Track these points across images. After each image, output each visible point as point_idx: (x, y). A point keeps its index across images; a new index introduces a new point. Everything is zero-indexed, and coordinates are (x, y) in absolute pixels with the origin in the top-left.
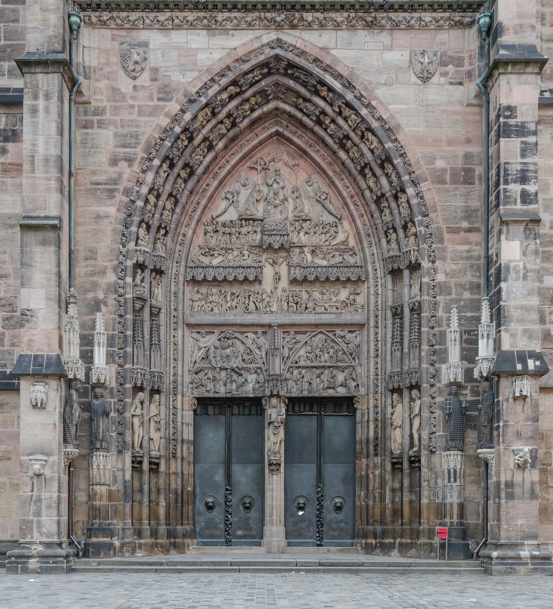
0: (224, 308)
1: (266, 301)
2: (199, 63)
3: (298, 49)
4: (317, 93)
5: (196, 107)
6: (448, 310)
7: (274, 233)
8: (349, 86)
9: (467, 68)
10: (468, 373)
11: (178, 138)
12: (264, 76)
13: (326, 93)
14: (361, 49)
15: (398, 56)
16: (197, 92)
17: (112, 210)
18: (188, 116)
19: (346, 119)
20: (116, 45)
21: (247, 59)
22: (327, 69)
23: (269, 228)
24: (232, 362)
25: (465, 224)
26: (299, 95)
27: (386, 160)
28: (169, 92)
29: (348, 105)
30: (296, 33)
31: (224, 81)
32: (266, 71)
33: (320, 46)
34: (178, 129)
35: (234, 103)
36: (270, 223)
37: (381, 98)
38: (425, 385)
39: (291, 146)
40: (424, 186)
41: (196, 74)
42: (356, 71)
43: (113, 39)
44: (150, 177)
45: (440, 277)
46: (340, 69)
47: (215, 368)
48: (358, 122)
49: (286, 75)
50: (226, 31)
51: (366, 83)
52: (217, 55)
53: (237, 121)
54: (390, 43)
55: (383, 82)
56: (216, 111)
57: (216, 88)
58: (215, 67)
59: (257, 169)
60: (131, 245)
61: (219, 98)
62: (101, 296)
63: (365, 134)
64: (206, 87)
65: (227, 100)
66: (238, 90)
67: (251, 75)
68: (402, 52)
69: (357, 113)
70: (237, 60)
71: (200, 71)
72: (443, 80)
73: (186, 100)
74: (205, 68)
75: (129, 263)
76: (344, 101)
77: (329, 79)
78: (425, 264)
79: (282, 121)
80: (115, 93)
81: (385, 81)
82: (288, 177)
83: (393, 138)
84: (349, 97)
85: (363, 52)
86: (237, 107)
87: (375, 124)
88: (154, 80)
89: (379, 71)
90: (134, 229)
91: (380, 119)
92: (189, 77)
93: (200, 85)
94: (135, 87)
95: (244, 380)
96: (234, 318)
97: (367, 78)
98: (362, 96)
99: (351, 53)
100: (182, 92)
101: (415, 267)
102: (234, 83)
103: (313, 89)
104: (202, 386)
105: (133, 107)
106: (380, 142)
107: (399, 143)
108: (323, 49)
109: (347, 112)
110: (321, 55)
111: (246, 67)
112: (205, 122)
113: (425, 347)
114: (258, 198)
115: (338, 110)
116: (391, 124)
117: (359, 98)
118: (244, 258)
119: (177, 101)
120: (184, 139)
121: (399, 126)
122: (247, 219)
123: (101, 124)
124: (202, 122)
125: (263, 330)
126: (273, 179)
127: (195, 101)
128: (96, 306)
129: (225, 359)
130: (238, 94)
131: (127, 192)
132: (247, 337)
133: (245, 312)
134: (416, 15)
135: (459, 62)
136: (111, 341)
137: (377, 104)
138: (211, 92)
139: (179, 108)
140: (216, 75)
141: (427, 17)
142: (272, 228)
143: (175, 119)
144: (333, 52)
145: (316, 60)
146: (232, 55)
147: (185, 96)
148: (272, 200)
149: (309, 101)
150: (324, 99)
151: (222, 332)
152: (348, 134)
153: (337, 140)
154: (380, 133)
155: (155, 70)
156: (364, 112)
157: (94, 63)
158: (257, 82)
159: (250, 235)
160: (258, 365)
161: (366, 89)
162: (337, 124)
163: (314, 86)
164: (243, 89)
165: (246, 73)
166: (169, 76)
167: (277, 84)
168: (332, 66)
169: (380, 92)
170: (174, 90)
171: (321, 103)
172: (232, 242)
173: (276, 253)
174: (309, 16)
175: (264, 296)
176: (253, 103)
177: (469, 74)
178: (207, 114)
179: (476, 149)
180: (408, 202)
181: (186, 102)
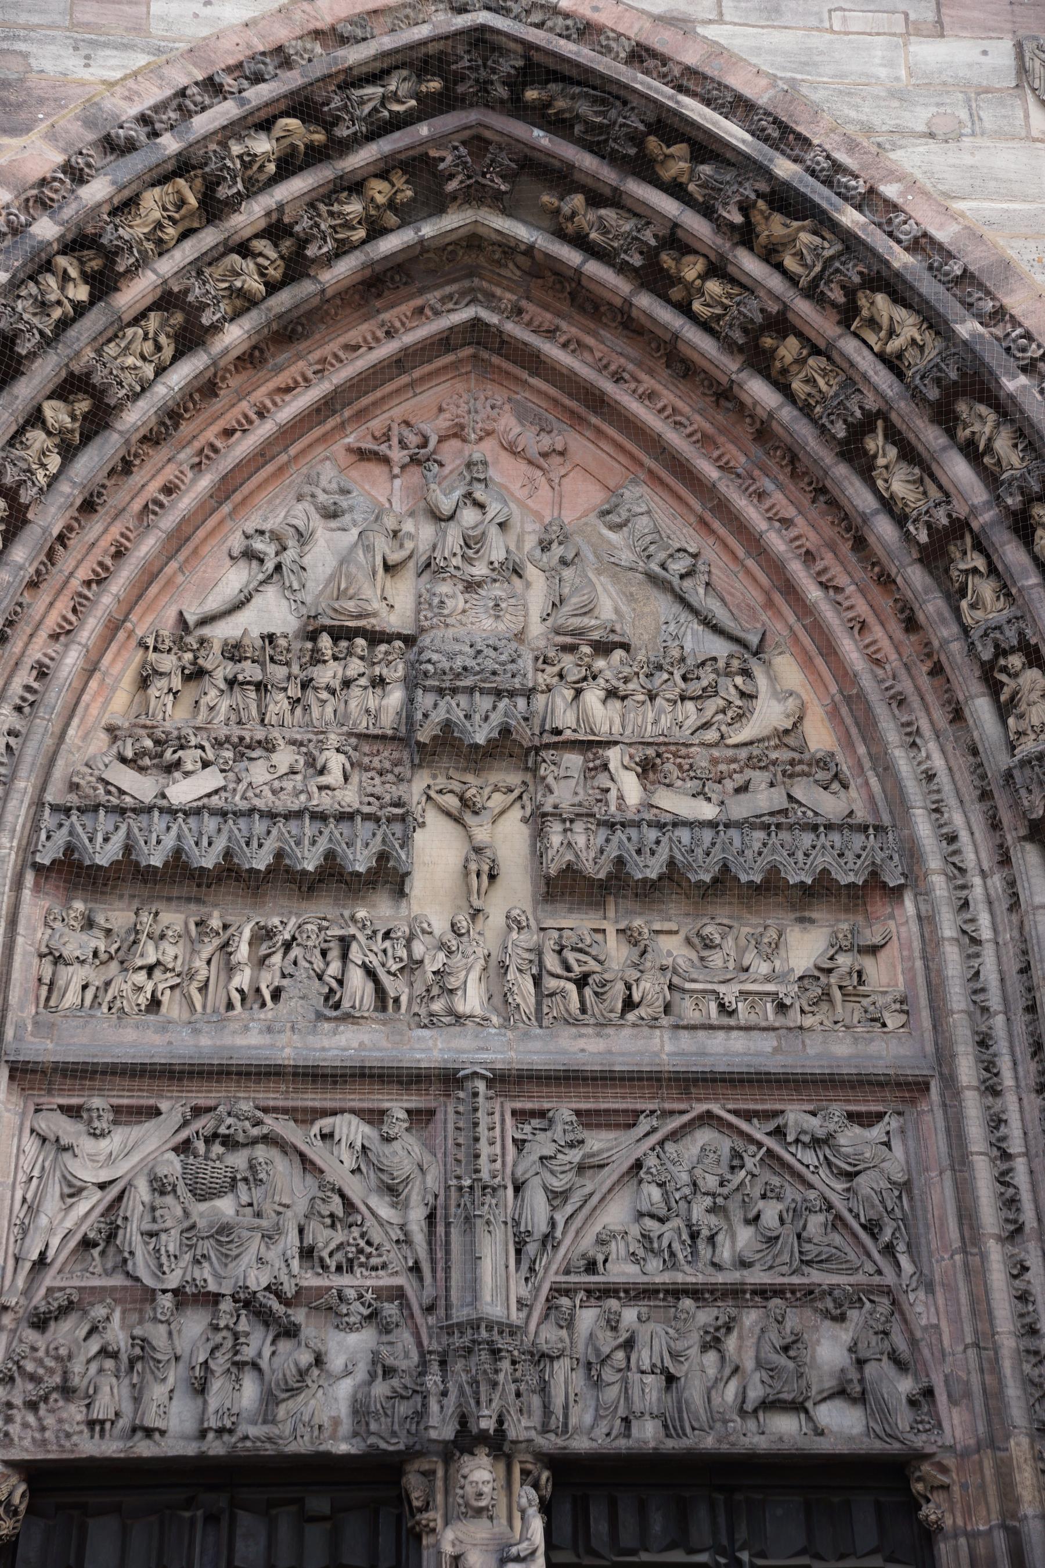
0: (216, 997)
1: (430, 967)
2: (157, 29)
3: (567, 16)
5: (136, 164)
7: (468, 682)
8: (785, 136)
11: (48, 266)
12: (430, 107)
13: (683, 165)
14: (818, 29)
16: (144, 119)
18: (97, 190)
19: (771, 256)
21: (359, 33)
22: (689, 80)
23: (445, 665)
24: (249, 1257)
28: (19, 106)
31: (259, 94)
32: (435, 85)
33: (656, 10)
34: (46, 229)
35: (298, 185)
36: (446, 647)
37: (918, 175)
39: (534, 381)
41: (141, 60)
42: (804, 91)
46: (739, 82)
47: (150, 1295)
48: (827, 253)
49: (517, 108)
51: (850, 129)
53: (311, 251)
54: (931, 16)
55: (922, 128)
56: (223, 192)
57: (226, 111)
58: (226, 44)
59: (386, 460)
61: (236, 149)
63: (863, 302)
64: (182, 105)
65: (272, 168)
66: (319, 137)
67: (373, 91)
68: (986, 44)
69: (824, 223)
70: (317, 34)
71: (159, 51)
73: (91, 136)
74: (183, 46)
76: (763, 187)
79: (498, 291)
81: (928, 124)
82: (521, 494)
83: (989, 306)
85: (828, 36)
86: (312, 205)
87: (901, 259)
89: (899, 95)
91: (922, 244)
92: (111, 66)
93: (153, 94)
95: (306, 1358)
96: (265, 1040)
97: (853, 114)
98: (838, 167)
100: (74, 108)
102: (302, 105)
103: (632, 151)
104: (67, 1391)
106: (934, 322)
107: (1015, 323)
109: (775, 226)
110: (662, 40)
111: (354, 55)
112: (171, 232)
114: (394, 558)
115: (738, 218)
116: (975, 258)
117: (831, 174)
118: (323, 780)
119: (52, 136)
120: (73, 273)
121: (1006, 265)
122: (337, 632)
124: (159, 226)
125: (415, 1102)
126: (457, 494)
127: (130, 147)
129: (205, 1246)
130: (315, 156)
132: (327, 1137)
133: (320, 1016)
137: (903, 194)
138: (203, 123)
139: (60, 159)
140: (229, 70)
142: (459, 663)
143: (40, 198)
144: (711, 32)
145: (640, 55)
146: (298, 16)
147: (89, 123)
148: (456, 561)
149: (615, 200)
150: (676, 190)
151: (198, 1111)
152: (786, 307)
153: (738, 337)
154: (928, 287)
158: (398, 123)
159: (355, 691)
160: (384, 1280)
161: (852, 146)
162: (733, 281)
163: (637, 139)
164: (342, 132)
165: (353, 79)
166: (25, 55)
167: (478, 143)
168: (708, 71)
169: (912, 158)
170: (41, 101)
172: (271, 718)
173: (477, 771)
175: (419, 949)
176: (380, 199)
178: (182, 203)
181: (93, 144)
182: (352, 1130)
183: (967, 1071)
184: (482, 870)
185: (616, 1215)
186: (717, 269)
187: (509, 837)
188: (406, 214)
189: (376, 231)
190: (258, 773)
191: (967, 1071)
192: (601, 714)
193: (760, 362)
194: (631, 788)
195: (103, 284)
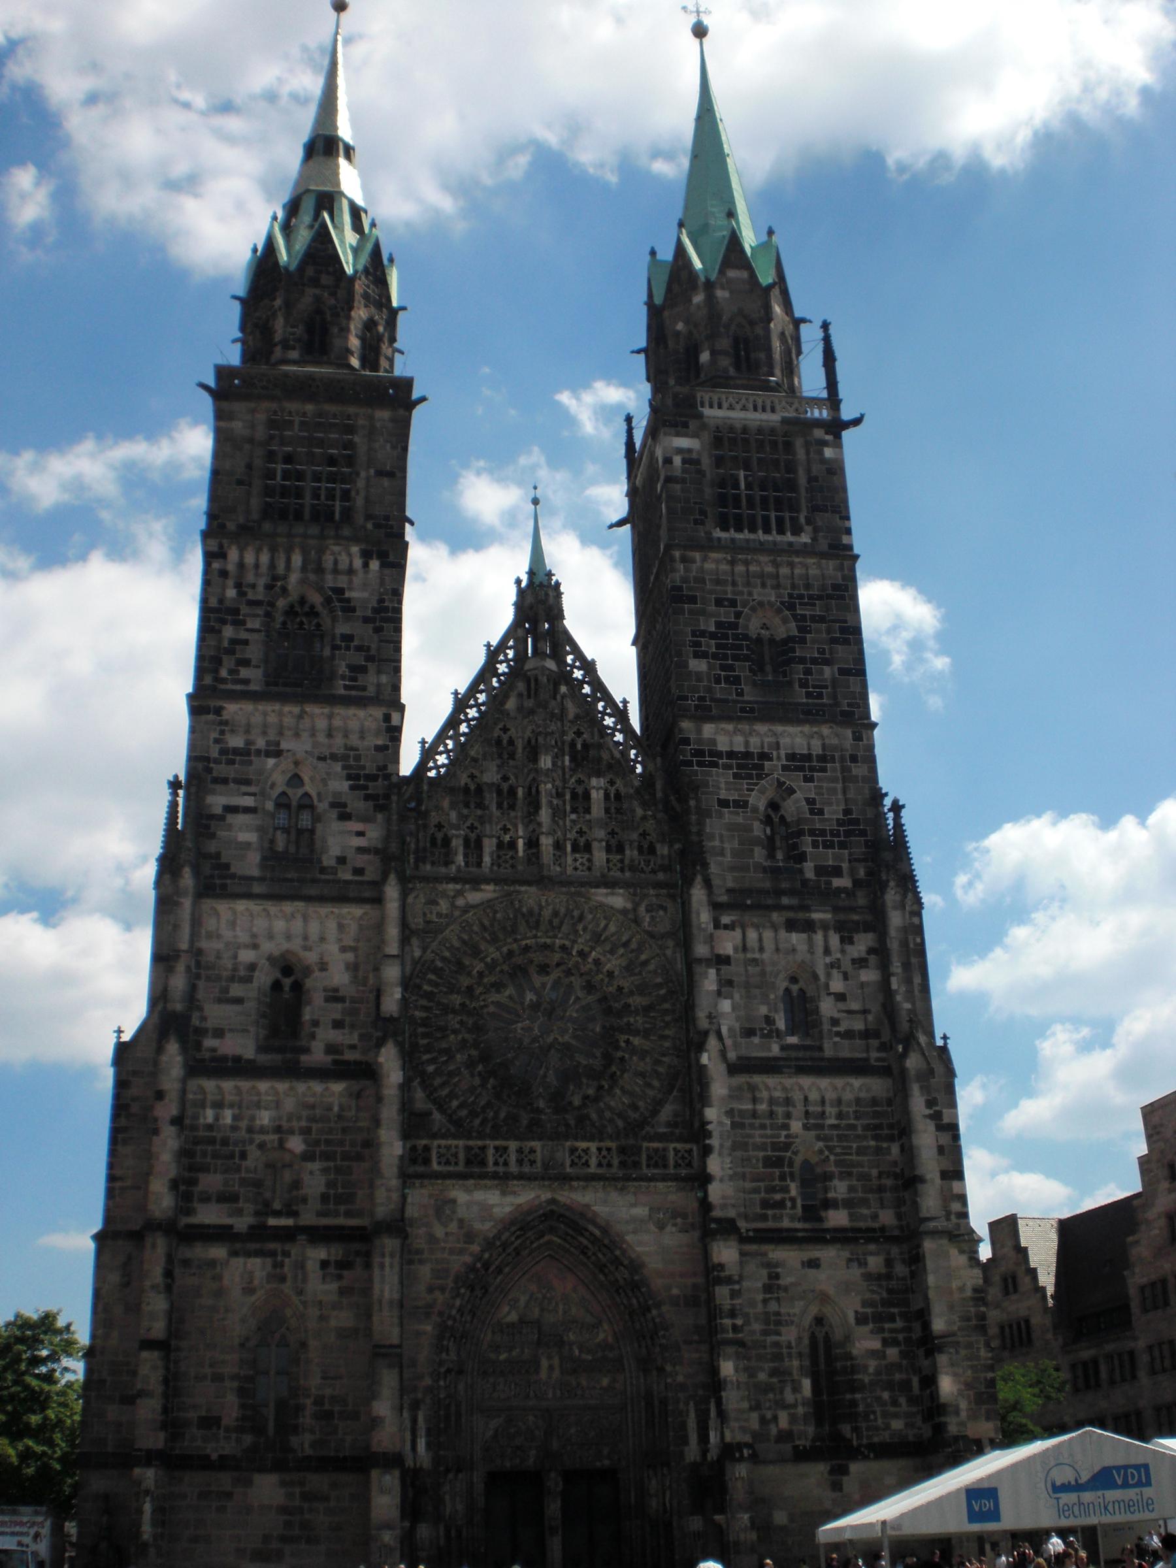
4: (582, 1235)
6: (687, 1404)
8: (605, 1231)
9: (690, 1220)
10: (704, 1452)
15: (641, 1211)
17: (429, 1328)
18: (486, 1256)
19: (604, 1255)
20: (432, 1202)
25: (696, 1337)
26: (567, 1234)
27: (635, 1286)
29: (605, 1246)
30: (566, 1193)
31: (513, 1229)
34: (479, 1265)
35: (519, 1241)
38: (673, 1464)
40: (664, 1308)
43: (430, 1196)
44: (458, 1302)
45: (680, 1379)
50: (514, 1193)
52: (508, 1209)
57: (507, 1234)
60: (444, 1356)
62: (420, 1395)
64: (500, 1233)
72: (674, 1229)
75: (442, 1370)
77: (591, 1228)
78: (668, 1368)
80: (432, 1239)
84: (606, 1242)
87: (626, 1262)
88: (461, 1227)
90: (445, 1343)
92: (488, 1225)
93: (495, 1231)
94: (447, 1234)
99: (607, 1209)
101: (661, 1370)
102: (521, 1229)
105: (444, 1248)
108: (587, 1206)
113: (671, 1434)
123: (421, 1262)
128: (415, 1406)
131: (441, 1314)
134: (652, 1184)
135: (684, 1216)
136: (429, 1432)
138: (504, 1238)
141: (660, 1185)
145: (582, 1215)
155: (461, 1221)
156: (618, 1253)
157: (416, 1215)
169: (628, 1238)
171: (585, 1242)
174: (575, 1184)
177: (693, 1225)
179: (700, 1280)
180: (653, 1319)
182: (531, 1418)
183: (629, 1408)
184: (551, 1368)
185: (573, 1430)
186: (594, 1254)
187: (556, 1361)
188: (538, 1239)
189: (532, 1243)
190: (514, 1353)
191: (629, 1408)
192: (572, 1337)
193: (601, 1271)
194: (577, 1352)
195: (487, 1270)
